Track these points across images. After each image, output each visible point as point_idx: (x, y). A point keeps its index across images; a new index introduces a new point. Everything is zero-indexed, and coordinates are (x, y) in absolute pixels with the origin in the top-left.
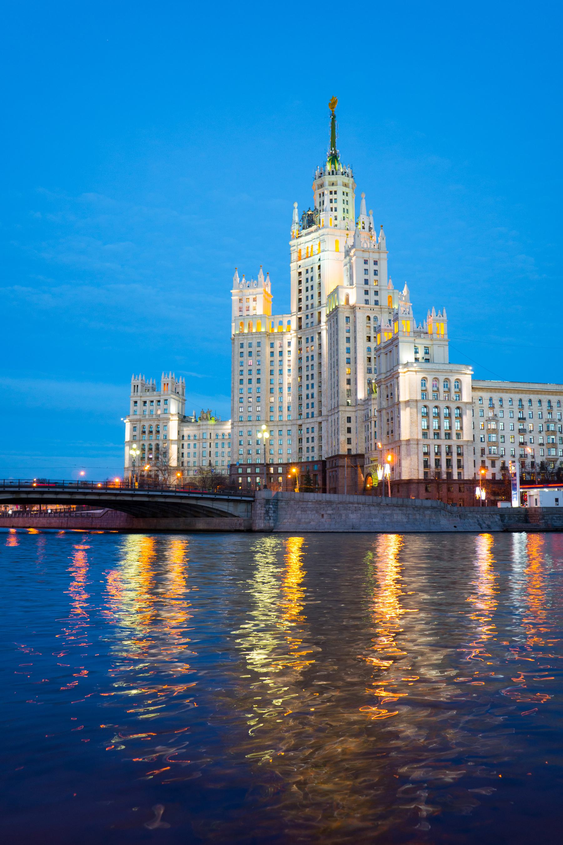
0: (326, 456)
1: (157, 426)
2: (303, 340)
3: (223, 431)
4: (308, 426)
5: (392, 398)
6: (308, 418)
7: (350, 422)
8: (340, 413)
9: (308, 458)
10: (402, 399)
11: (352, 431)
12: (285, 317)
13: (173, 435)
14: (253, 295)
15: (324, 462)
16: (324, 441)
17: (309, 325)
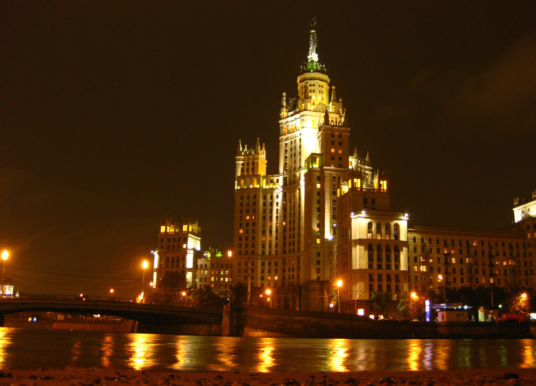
5: (347, 237)
6: (290, 252)
11: (320, 263)
15: (301, 287)
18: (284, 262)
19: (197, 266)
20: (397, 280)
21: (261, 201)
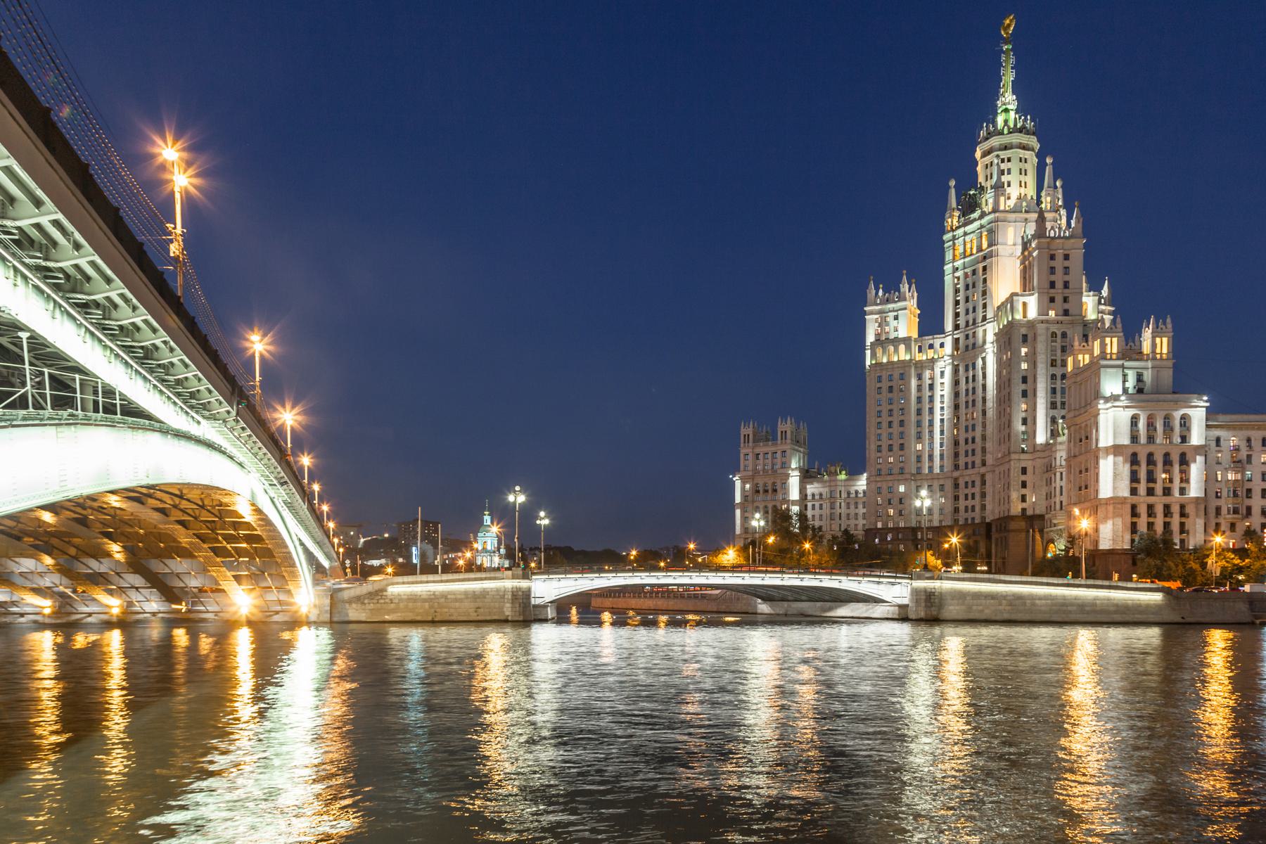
0: (992, 518)
2: (961, 369)
3: (856, 488)
4: (967, 479)
6: (966, 468)
7: (1025, 474)
8: (1012, 463)
9: (966, 519)
10: (1102, 444)
13: (794, 494)
14: (894, 311)
15: (989, 525)
16: (989, 498)
18: (956, 486)
19: (806, 495)
21: (914, 383)
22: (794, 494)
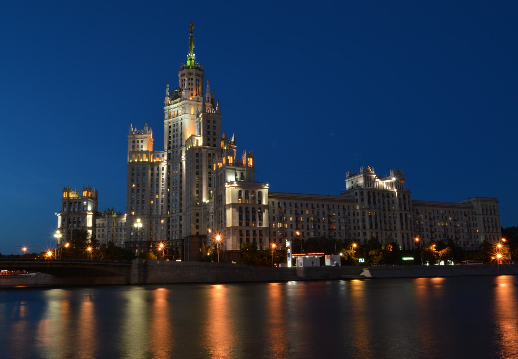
0: (184, 237)
1: (79, 218)
10: (227, 203)
12: (160, 152)
13: (90, 224)
14: (141, 138)
15: (183, 240)
16: (183, 227)
17: (175, 158)
19: (96, 224)
20: (261, 235)
21: (150, 172)
22: (90, 224)
